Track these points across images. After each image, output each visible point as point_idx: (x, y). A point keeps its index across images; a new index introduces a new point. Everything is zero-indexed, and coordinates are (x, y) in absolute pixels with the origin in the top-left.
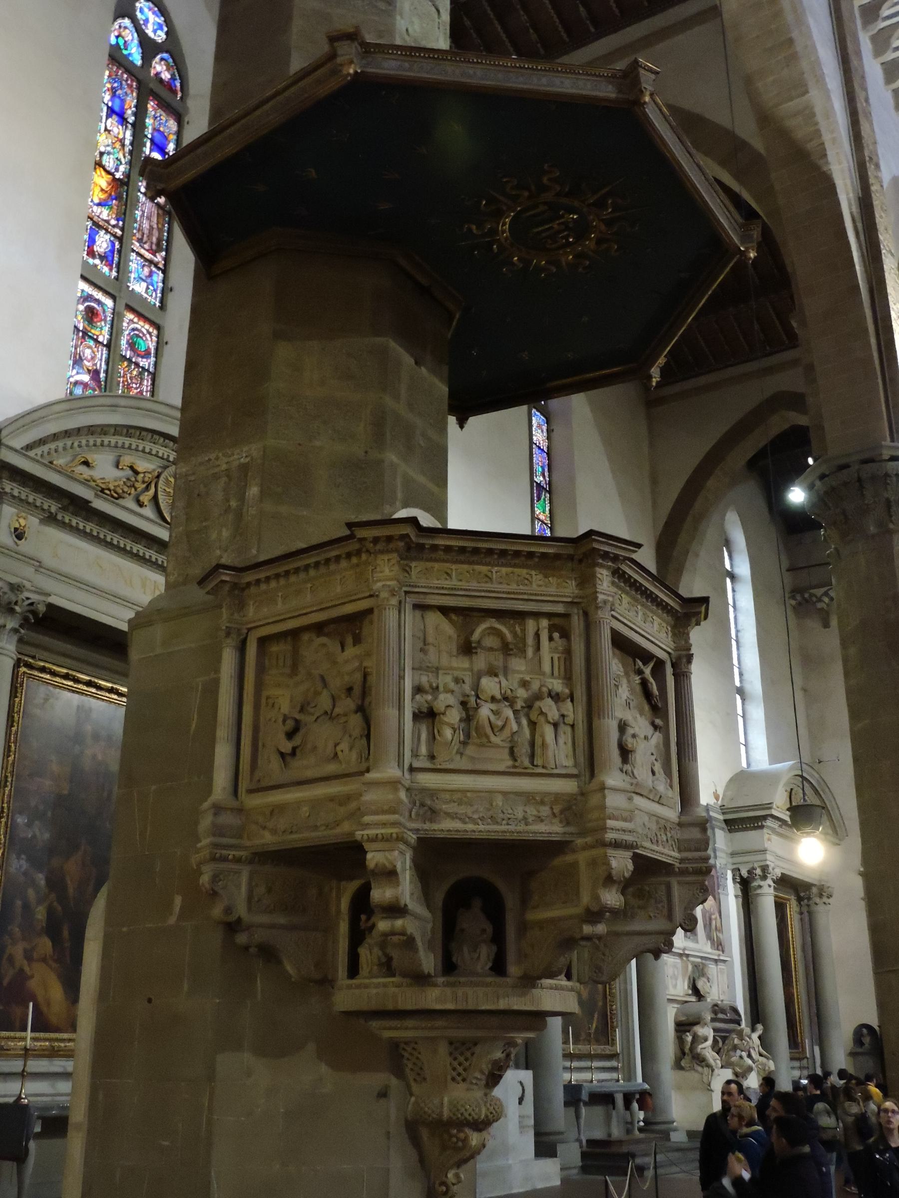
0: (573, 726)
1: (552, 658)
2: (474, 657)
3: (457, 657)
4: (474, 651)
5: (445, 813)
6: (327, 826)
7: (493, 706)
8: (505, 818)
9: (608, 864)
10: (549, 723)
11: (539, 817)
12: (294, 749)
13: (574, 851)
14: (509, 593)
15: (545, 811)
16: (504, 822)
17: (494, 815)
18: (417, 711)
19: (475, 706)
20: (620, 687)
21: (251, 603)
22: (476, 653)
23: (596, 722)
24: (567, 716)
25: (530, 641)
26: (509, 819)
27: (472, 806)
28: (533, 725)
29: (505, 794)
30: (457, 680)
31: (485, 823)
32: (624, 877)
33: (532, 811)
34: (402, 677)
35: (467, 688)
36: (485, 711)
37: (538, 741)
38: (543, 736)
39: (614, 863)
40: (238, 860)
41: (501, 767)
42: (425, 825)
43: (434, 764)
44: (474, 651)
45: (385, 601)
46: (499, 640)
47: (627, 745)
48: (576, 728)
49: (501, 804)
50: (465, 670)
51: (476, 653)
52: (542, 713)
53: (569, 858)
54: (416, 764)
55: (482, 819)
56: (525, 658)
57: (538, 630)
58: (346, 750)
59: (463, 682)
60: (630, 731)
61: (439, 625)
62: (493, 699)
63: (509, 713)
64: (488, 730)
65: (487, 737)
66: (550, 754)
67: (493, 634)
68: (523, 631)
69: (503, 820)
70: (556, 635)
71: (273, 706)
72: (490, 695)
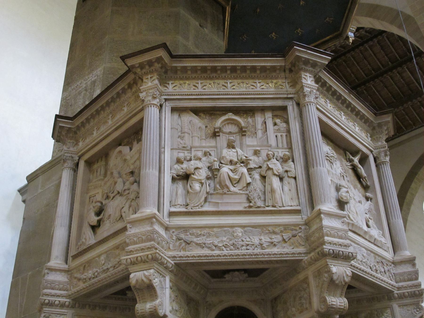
0: (295, 178)
1: (276, 136)
2: (218, 138)
3: (205, 140)
4: (217, 134)
5: (197, 244)
6: (115, 266)
7: (232, 167)
8: (244, 244)
9: (329, 272)
10: (275, 175)
11: (272, 243)
12: (99, 222)
13: (304, 269)
14: (240, 94)
15: (277, 238)
16: (244, 248)
17: (235, 243)
18: (175, 175)
19: (218, 168)
20: (334, 164)
21: (81, 140)
22: (219, 136)
23: (311, 170)
24: (290, 171)
25: (259, 126)
26: (248, 245)
27: (217, 237)
28: (263, 178)
29: (243, 227)
30: (206, 154)
31: (228, 249)
32: (344, 281)
33: (265, 239)
34: (161, 153)
35: (213, 158)
36: (226, 169)
37: (268, 188)
38: (271, 185)
39: (334, 269)
40: (62, 305)
41: (241, 208)
42: (181, 253)
43: (187, 208)
44: (217, 134)
45: (148, 102)
46: (236, 127)
47: (342, 198)
48: (297, 178)
49: (240, 234)
50: (212, 147)
51: (219, 136)
52: (269, 169)
53: (301, 276)
54: (173, 209)
55: (226, 246)
56: (256, 137)
57: (265, 119)
58: (127, 211)
59: (210, 155)
60: (344, 190)
61: (191, 121)
62: (231, 162)
63: (245, 170)
64: (228, 183)
65: (228, 187)
66: (277, 196)
67: (231, 123)
68: (254, 121)
69: (243, 246)
70: (278, 121)
71: (92, 202)
72: (229, 160)
